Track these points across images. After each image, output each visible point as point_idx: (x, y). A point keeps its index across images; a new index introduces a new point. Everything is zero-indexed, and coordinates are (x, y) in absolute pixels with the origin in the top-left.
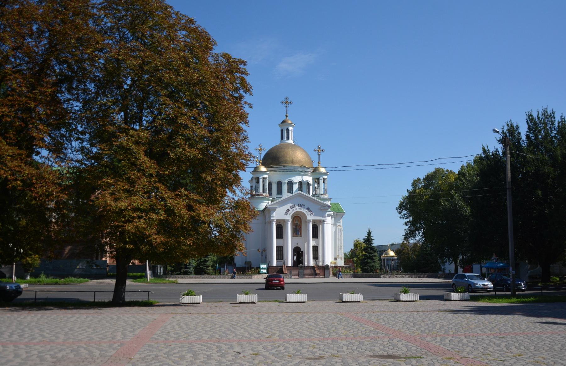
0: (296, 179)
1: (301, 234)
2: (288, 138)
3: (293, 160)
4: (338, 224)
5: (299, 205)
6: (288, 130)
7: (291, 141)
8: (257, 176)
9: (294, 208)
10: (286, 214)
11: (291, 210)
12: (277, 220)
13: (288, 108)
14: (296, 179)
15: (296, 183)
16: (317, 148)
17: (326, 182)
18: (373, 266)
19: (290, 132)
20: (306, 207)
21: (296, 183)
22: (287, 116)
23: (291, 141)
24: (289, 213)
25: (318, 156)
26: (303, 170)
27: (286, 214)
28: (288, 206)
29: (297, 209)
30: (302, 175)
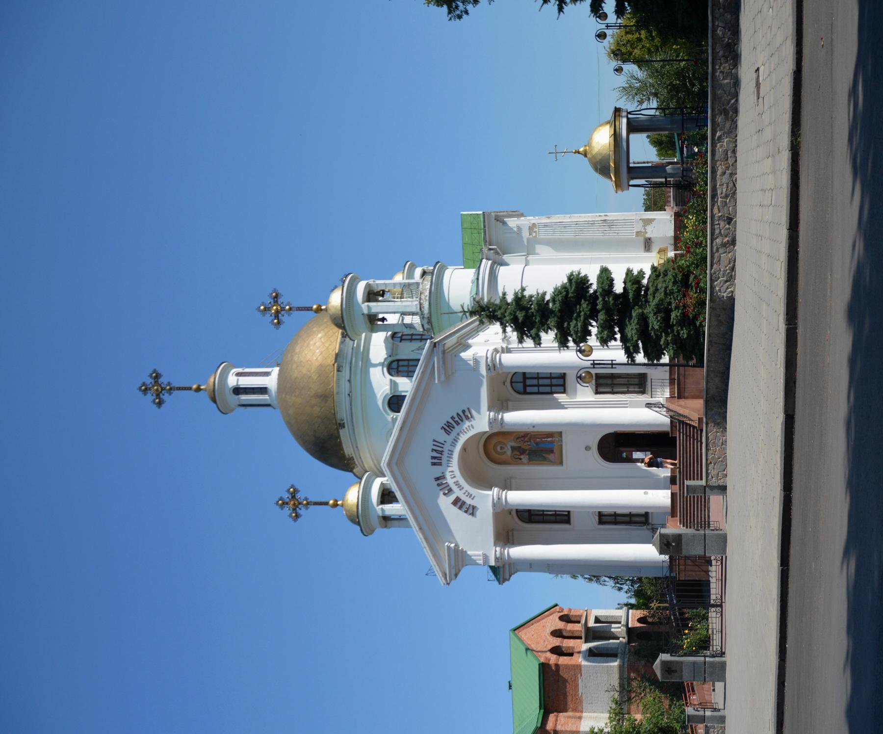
0: (381, 383)
1: (550, 435)
2: (263, 390)
3: (317, 396)
4: (526, 234)
5: (437, 461)
6: (238, 391)
7: (271, 381)
8: (375, 522)
9: (450, 481)
10: (471, 511)
11: (457, 493)
12: (495, 545)
13: (176, 384)
14: (381, 383)
15: (394, 385)
16: (268, 318)
17: (379, 283)
18: (664, 311)
19: (245, 382)
20: (442, 436)
21: (394, 385)
22: (198, 389)
23: (271, 381)
24: (469, 501)
25: (295, 313)
26: (349, 362)
27: (471, 511)
28: (445, 503)
29: (453, 472)
30: (367, 364)
